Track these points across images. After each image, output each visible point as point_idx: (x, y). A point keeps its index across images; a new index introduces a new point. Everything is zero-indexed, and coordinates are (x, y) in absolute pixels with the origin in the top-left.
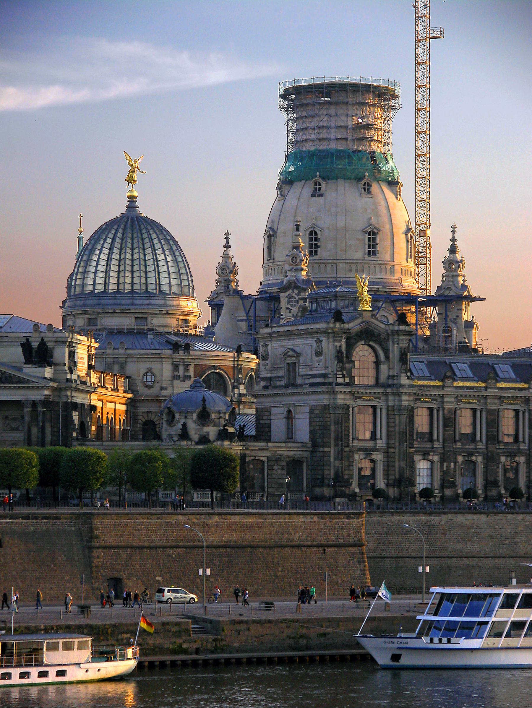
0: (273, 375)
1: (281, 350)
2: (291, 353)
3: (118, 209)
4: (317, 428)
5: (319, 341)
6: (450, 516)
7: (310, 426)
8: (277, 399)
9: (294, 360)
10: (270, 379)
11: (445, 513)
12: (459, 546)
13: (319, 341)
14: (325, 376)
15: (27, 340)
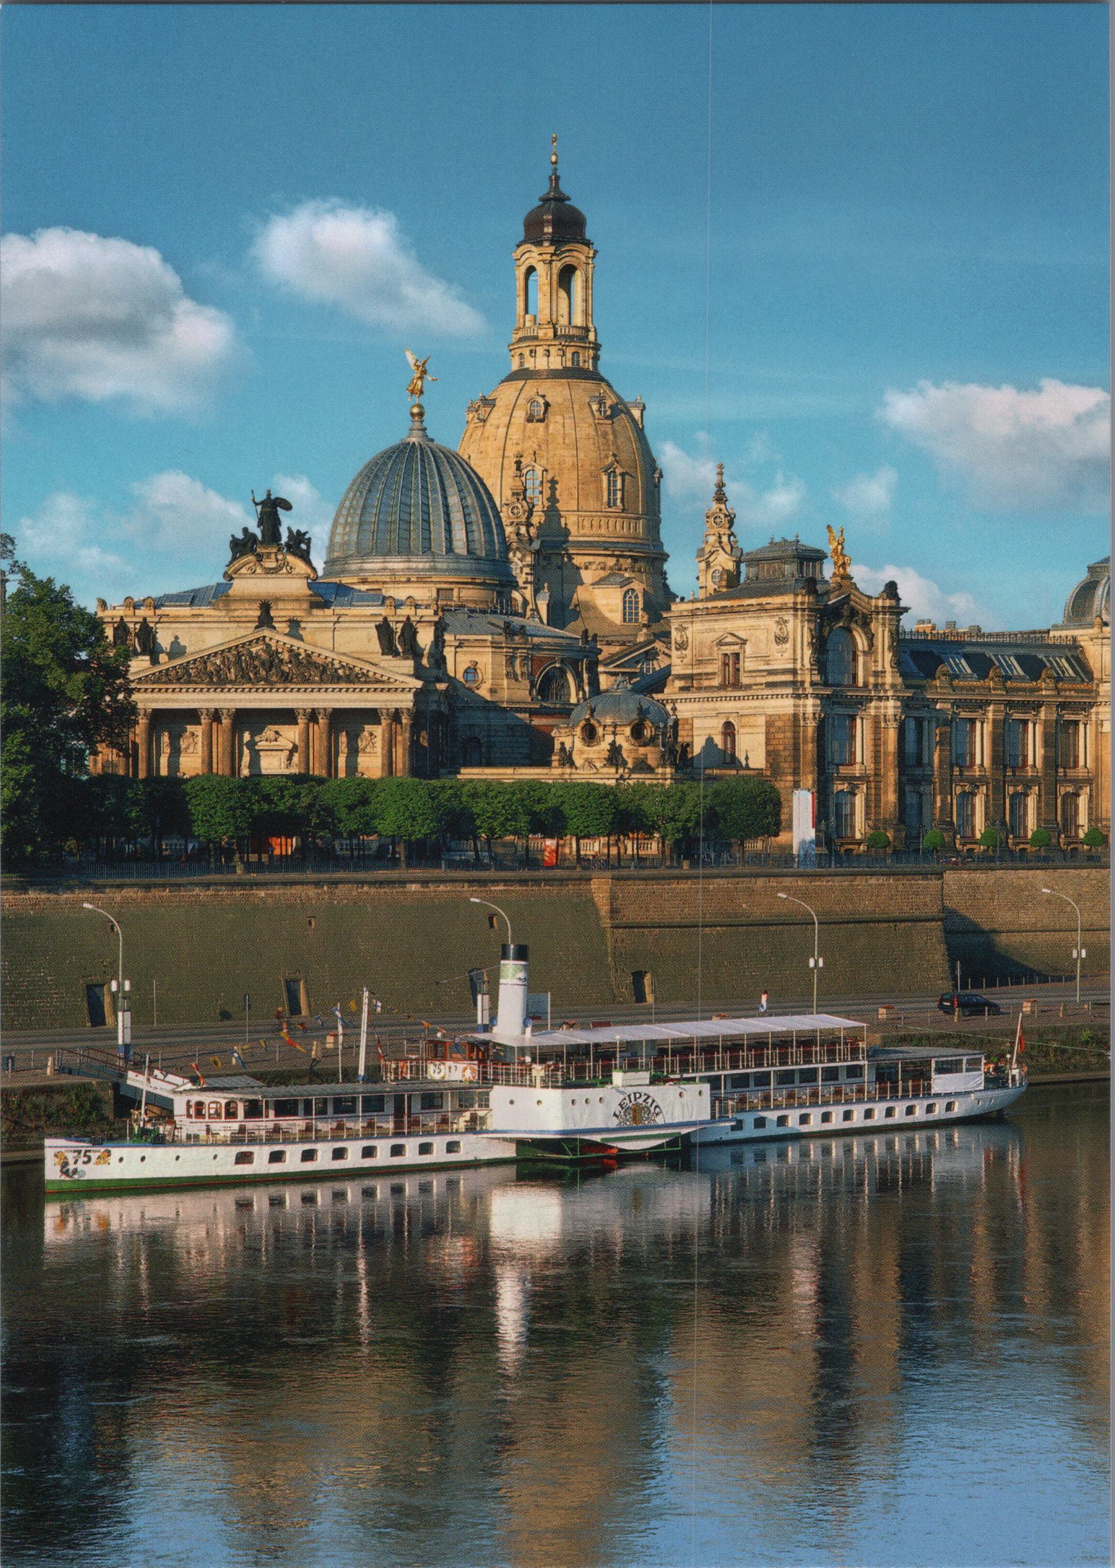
0: (695, 672)
1: (711, 637)
2: (730, 639)
3: (397, 431)
4: (781, 748)
5: (782, 622)
6: (999, 873)
7: (767, 744)
8: (707, 705)
9: (736, 648)
10: (691, 677)
11: (992, 869)
12: (1009, 916)
13: (782, 622)
14: (794, 672)
15: (385, 619)
